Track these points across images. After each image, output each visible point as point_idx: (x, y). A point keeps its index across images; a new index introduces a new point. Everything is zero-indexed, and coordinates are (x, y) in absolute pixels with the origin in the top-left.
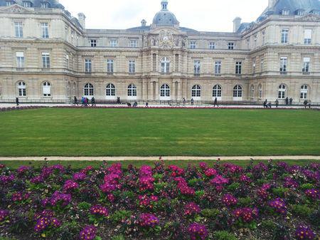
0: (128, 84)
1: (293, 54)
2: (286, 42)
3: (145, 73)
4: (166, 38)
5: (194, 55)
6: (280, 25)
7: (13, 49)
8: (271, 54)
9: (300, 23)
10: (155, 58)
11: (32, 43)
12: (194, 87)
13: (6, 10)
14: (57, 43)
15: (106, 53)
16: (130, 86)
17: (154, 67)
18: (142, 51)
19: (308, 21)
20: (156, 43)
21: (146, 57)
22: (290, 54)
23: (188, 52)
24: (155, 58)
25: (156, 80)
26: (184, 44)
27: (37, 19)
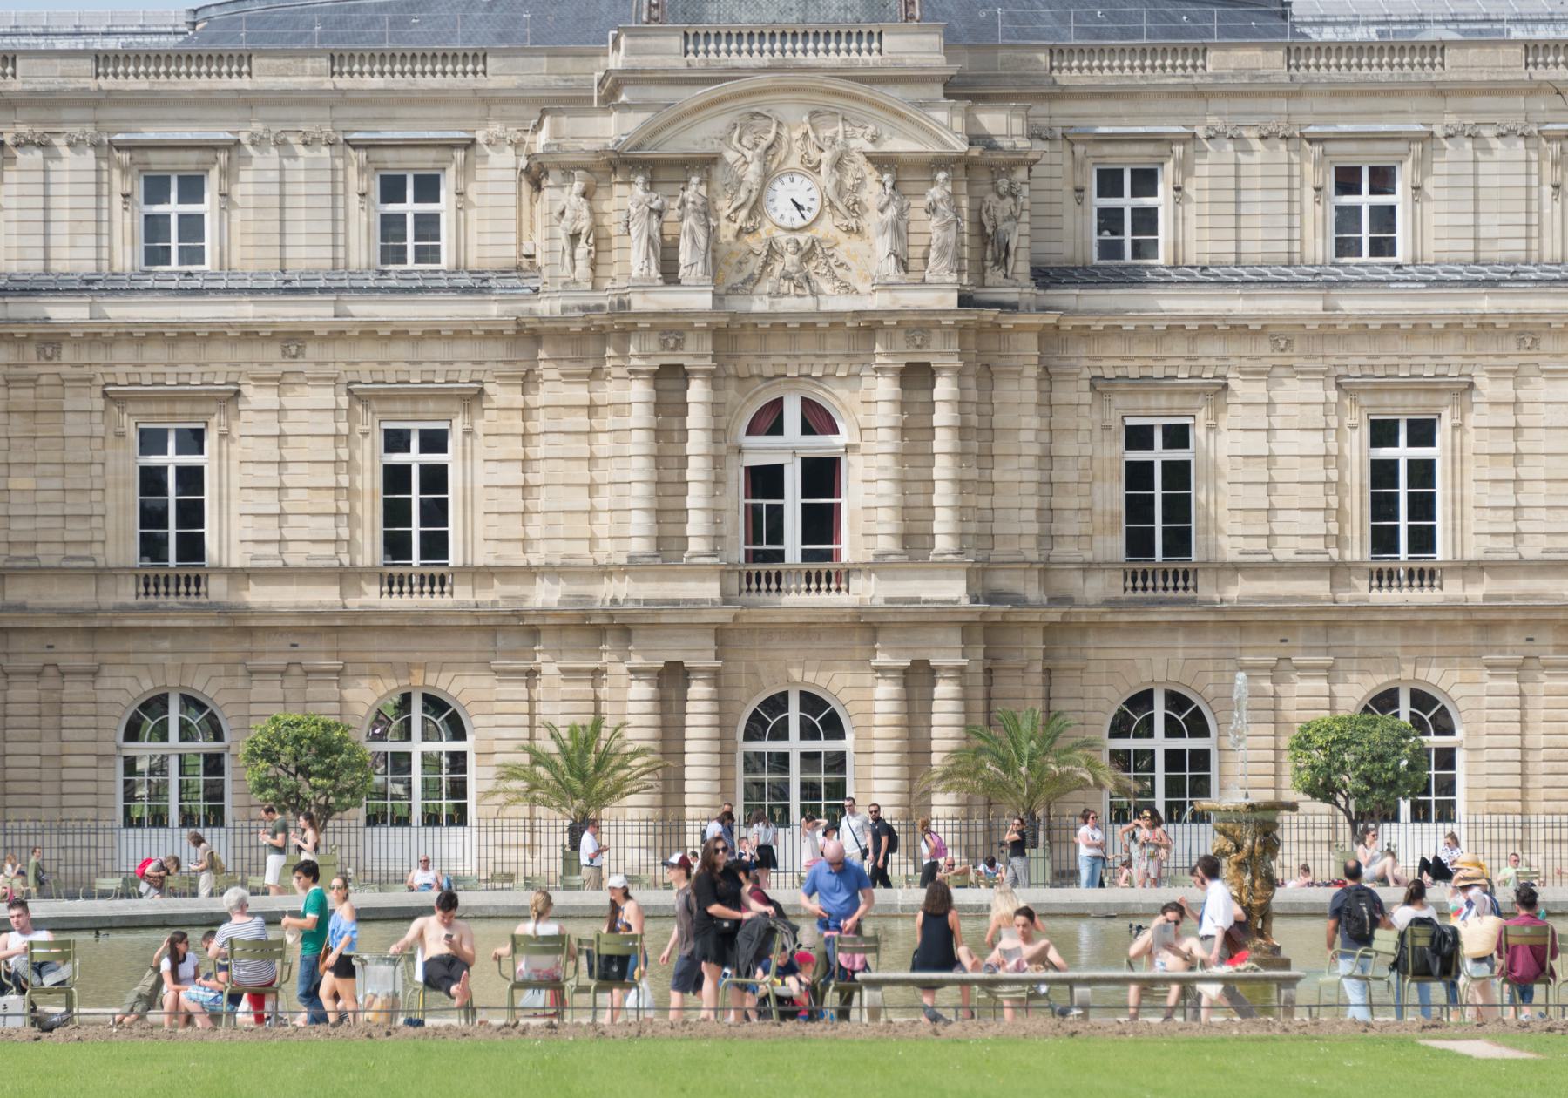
5: (1114, 360)
15: (122, 366)
18: (529, 335)
21: (579, 393)
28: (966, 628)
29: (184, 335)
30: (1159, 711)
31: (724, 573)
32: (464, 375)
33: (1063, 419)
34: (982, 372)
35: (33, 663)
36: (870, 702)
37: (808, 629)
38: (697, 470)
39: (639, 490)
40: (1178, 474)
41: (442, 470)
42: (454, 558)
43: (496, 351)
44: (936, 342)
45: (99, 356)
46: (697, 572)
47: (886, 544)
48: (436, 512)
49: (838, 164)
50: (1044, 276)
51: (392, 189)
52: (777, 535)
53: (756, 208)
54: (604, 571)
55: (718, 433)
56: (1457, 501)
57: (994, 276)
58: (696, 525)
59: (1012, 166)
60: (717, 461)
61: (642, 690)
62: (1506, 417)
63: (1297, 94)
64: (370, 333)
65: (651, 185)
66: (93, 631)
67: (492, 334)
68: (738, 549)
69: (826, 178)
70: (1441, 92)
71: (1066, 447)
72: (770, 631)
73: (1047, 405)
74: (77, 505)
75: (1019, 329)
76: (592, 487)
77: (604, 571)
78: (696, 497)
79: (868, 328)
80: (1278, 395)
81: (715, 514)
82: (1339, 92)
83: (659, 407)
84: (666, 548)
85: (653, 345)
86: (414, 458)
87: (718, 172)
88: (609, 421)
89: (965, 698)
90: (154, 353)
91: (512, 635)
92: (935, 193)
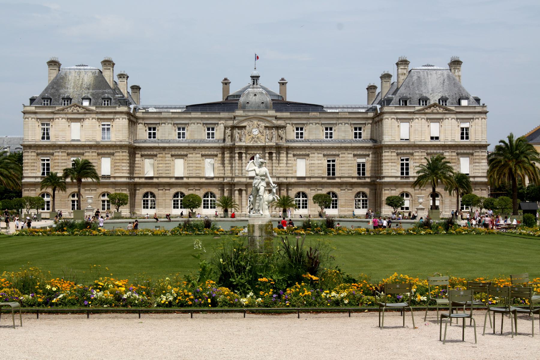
1: (417, 154)
3: (227, 177)
4: (255, 132)
6: (397, 119)
7: (68, 154)
8: (387, 154)
9: (423, 116)
10: (240, 157)
11: (90, 147)
13: (63, 110)
14: (121, 147)
16: (206, 195)
18: (223, 149)
19: (432, 113)
20: (243, 139)
21: (228, 155)
22: (412, 154)
24: (240, 157)
26: (280, 137)
27: (98, 119)
29: (181, 148)
32: (215, 153)
33: (289, 159)
50: (287, 141)
57: (280, 141)
61: (237, 192)
64: (204, 148)
67: (219, 148)
70: (338, 118)
73: (287, 157)
74: (167, 168)
77: (232, 178)
79: (264, 148)
83: (239, 157)
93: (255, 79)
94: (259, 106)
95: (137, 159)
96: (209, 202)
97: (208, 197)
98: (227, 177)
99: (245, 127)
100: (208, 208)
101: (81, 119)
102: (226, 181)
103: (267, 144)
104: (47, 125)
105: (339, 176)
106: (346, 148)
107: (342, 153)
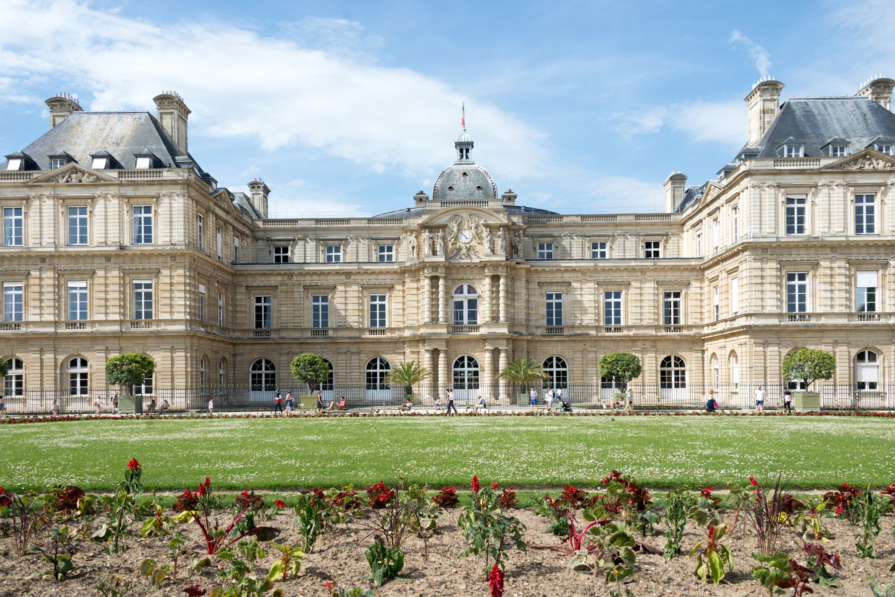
0: (366, 359)
2: (801, 230)
3: (408, 328)
5: (544, 278)
7: (60, 275)
11: (108, 257)
12: (548, 363)
14: (173, 257)
15: (308, 280)
16: (372, 364)
17: (434, 312)
18: (403, 272)
21: (415, 285)
23: (528, 271)
25: (442, 347)
28: (508, 339)
30: (554, 362)
31: (448, 327)
32: (389, 282)
33: (531, 292)
34: (512, 280)
35: (285, 351)
36: (484, 359)
37: (469, 341)
38: (441, 301)
39: (427, 306)
40: (559, 305)
41: (384, 305)
42: (387, 326)
43: (396, 277)
44: (500, 269)
45: (302, 279)
46: (441, 326)
47: (488, 319)
48: (383, 315)
49: (476, 227)
51: (382, 249)
52: (462, 318)
53: (456, 238)
54: (420, 327)
55: (447, 293)
56: (626, 311)
57: (515, 256)
58: (441, 314)
59: (519, 230)
60: (446, 300)
61: (427, 355)
62: (638, 291)
63: (583, 226)
64: (366, 272)
65: (430, 232)
66: (301, 343)
67: (395, 273)
68: (452, 321)
69: (473, 231)
70: (616, 225)
71: (532, 299)
72: (459, 341)
73: (528, 289)
75: (521, 268)
76: (418, 308)
77: (420, 327)
78: (441, 308)
79: (483, 266)
80: (583, 286)
81: (446, 313)
82: (593, 226)
84: (434, 320)
85: (430, 270)
86: (378, 302)
87: (447, 229)
88: (421, 290)
89: (507, 357)
90: (315, 278)
91: (398, 344)
92: (500, 233)
93: (464, 148)
94: (471, 194)
95: (238, 297)
96: (378, 378)
97: (375, 368)
98: (408, 328)
99: (444, 227)
100: (375, 388)
101: (87, 198)
102: (407, 333)
103: (487, 259)
104: (18, 211)
105: (630, 324)
106: (643, 271)
107: (636, 281)
